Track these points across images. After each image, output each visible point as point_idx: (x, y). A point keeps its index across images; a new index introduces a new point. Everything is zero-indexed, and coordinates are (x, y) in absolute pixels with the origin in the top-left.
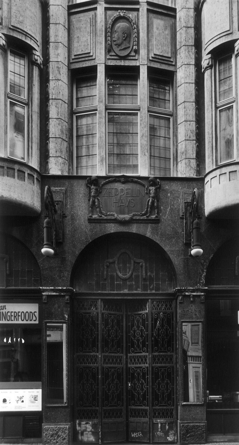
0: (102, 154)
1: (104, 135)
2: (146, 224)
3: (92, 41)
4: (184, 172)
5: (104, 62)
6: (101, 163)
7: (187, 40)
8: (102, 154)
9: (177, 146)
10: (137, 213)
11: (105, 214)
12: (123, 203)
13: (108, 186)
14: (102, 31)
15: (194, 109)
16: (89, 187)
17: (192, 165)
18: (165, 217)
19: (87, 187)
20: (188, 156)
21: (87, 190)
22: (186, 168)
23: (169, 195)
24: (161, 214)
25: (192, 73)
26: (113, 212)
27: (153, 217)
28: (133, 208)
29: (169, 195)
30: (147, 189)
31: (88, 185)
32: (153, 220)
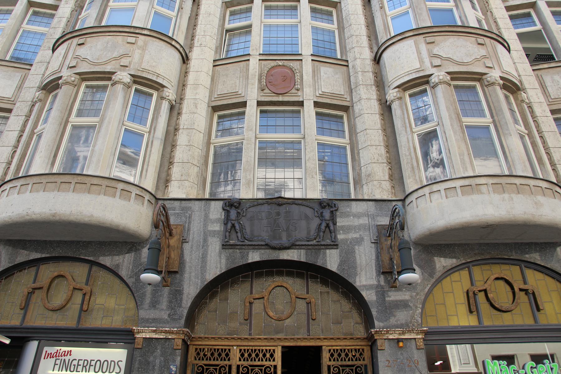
0: (248, 177)
1: (253, 159)
3: (241, 84)
5: (256, 98)
7: (363, 80)
8: (248, 177)
14: (255, 76)
15: (381, 135)
17: (384, 187)
19: (224, 209)
25: (375, 106)
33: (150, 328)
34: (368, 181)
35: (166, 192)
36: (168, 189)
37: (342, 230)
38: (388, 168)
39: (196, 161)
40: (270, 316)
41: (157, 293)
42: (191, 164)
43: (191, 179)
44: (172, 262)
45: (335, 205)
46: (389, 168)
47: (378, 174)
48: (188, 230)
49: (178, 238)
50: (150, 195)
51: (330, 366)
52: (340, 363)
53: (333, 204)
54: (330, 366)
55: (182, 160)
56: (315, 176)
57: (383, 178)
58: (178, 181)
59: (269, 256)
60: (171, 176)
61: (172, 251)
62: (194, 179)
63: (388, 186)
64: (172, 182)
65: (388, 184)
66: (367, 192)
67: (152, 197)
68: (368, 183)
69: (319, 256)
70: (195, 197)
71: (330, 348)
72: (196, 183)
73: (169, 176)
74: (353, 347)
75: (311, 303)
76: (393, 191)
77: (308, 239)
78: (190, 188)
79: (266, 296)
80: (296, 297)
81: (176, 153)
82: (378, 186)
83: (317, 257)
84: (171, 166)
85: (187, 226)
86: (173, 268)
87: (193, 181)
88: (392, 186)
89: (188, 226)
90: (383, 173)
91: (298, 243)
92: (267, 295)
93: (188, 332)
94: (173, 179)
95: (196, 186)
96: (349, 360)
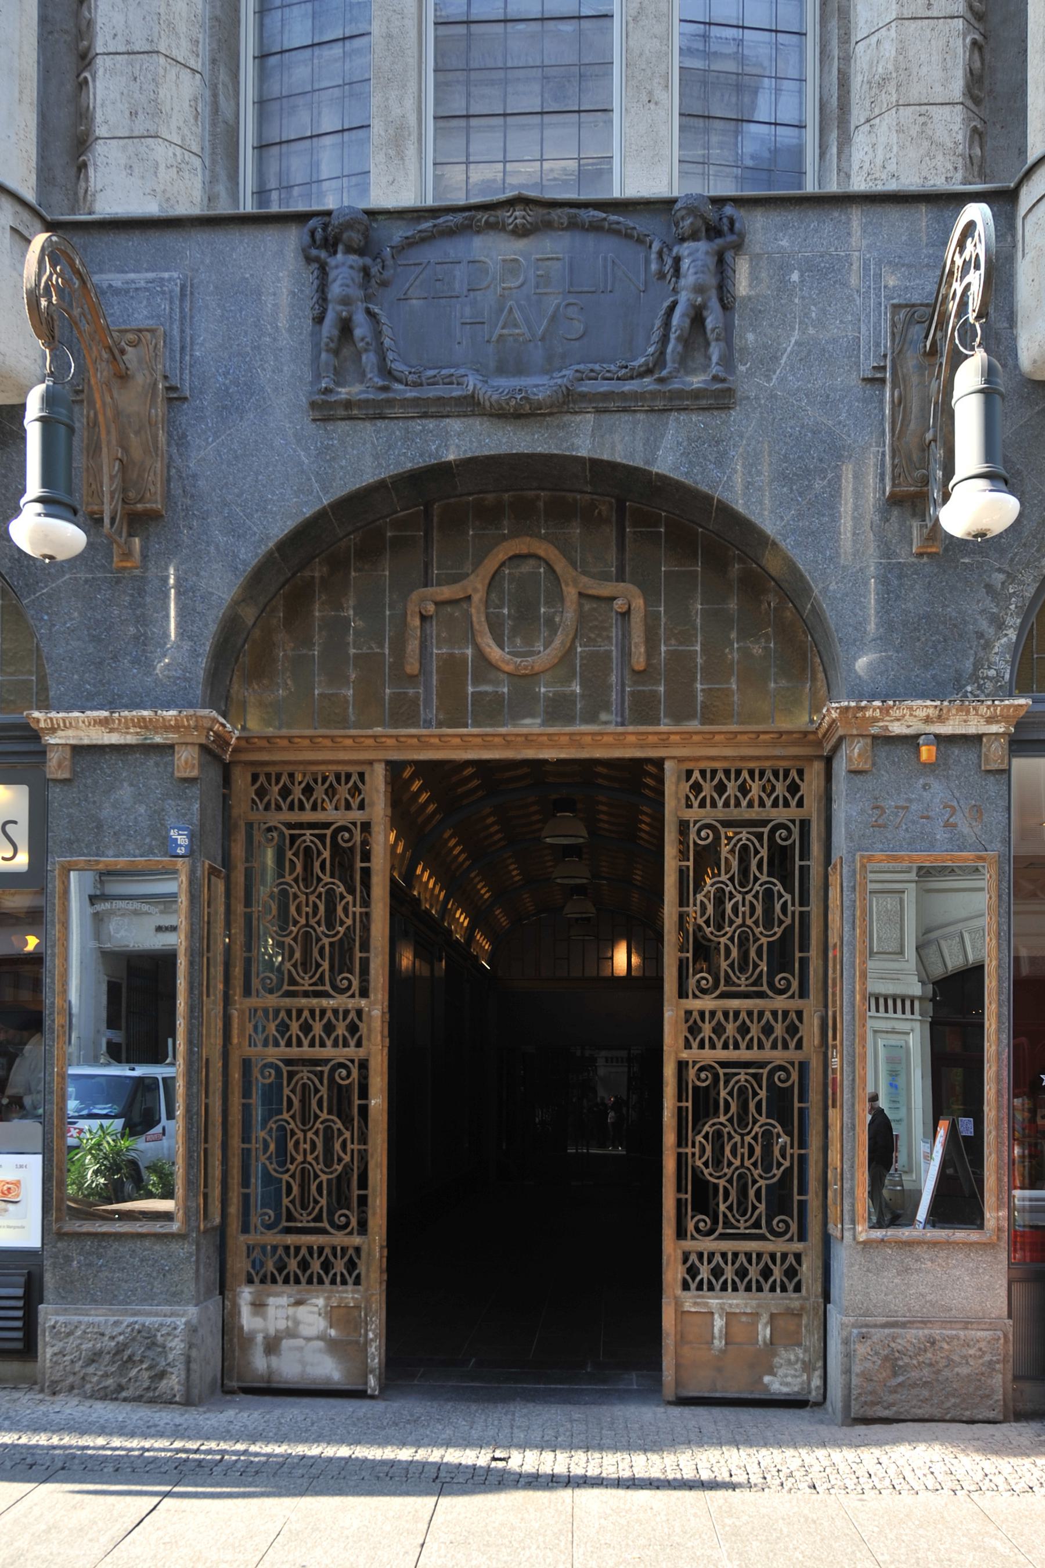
0: (396, 111)
1: (411, 25)
2: (653, 418)
4: (892, 167)
6: (392, 153)
8: (396, 111)
9: (846, 59)
10: (597, 367)
11: (410, 378)
12: (516, 326)
13: (431, 253)
16: (317, 260)
17: (941, 134)
18: (769, 379)
19: (309, 260)
20: (916, 92)
21: (309, 276)
22: (902, 147)
23: (795, 277)
24: (742, 368)
26: (457, 366)
27: (697, 381)
28: (577, 344)
29: (795, 277)
30: (660, 254)
31: (314, 252)
32: (697, 394)
33: (88, 713)
34: (877, 112)
35: (81, 192)
36: (87, 180)
37: (754, 331)
38: (968, 40)
39: (185, 43)
40: (493, 661)
41: (99, 593)
42: (162, 60)
43: (173, 125)
44: (135, 476)
45: (732, 222)
46: (974, 43)
47: (924, 70)
48: (183, 348)
49: (148, 381)
50: (19, 208)
51: (688, 822)
52: (721, 813)
53: (725, 220)
54: (688, 822)
55: (128, 42)
56: (661, 95)
57: (939, 94)
58: (122, 142)
59: (479, 441)
60: (93, 119)
61: (132, 435)
62: (186, 131)
63: (956, 128)
64: (100, 148)
65: (959, 119)
66: (867, 159)
67: (26, 216)
68: (877, 120)
69: (663, 436)
70: (196, 211)
71: (690, 765)
72: (195, 148)
73: (84, 121)
74: (767, 764)
75: (632, 612)
76: (978, 151)
77: (624, 371)
78: (175, 169)
79: (475, 590)
80: (580, 594)
81: (96, 6)
82: (914, 131)
83: (655, 441)
84: (87, 74)
85: (176, 332)
86: (140, 501)
87: (183, 139)
88: (975, 130)
89: (182, 331)
90: (945, 69)
91: (586, 387)
92: (479, 586)
93: (215, 720)
94: (101, 131)
95: (197, 162)
96: (750, 805)
